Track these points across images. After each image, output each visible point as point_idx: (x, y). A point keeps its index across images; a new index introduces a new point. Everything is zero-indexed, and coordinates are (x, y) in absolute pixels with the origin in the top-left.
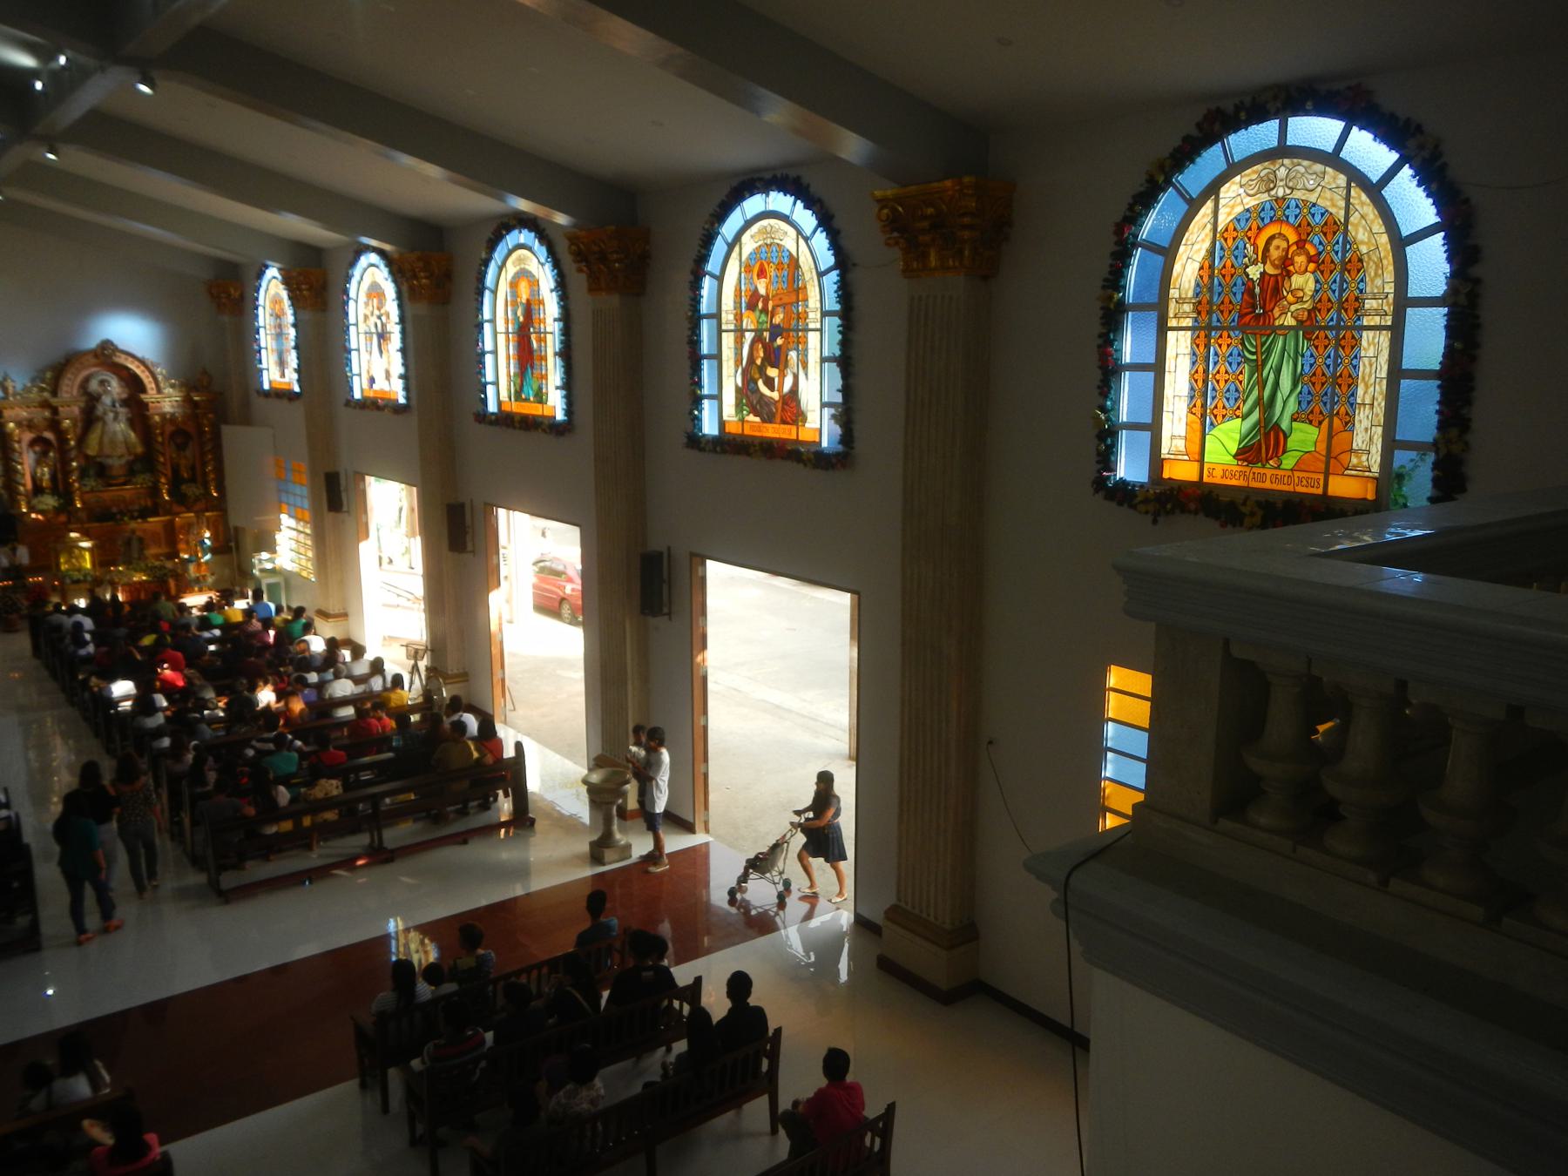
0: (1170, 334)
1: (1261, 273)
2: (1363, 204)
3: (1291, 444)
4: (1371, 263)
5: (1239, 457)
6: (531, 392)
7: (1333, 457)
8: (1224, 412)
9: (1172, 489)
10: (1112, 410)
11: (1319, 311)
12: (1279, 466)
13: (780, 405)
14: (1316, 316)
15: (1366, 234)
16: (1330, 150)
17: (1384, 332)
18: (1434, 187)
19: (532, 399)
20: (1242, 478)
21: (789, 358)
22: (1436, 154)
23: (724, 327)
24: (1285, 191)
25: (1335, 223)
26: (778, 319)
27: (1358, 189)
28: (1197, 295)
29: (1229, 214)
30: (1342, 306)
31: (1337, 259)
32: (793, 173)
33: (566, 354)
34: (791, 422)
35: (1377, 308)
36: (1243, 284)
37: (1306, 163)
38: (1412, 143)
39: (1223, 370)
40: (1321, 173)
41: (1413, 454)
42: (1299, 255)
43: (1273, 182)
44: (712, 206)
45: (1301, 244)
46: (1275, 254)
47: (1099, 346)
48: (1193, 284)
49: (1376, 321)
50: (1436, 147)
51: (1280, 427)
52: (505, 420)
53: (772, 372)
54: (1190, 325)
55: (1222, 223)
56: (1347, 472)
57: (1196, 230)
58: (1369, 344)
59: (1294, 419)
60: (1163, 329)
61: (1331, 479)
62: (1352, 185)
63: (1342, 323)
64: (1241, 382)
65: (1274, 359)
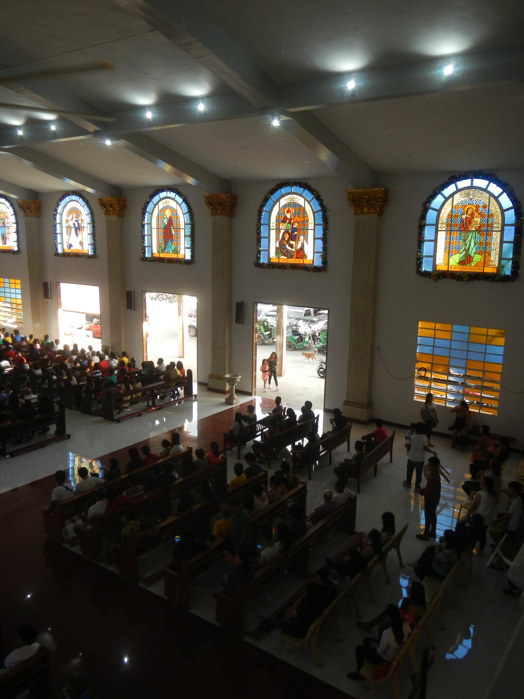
0: (439, 232)
1: (466, 217)
2: (493, 201)
3: (473, 260)
6: (170, 250)
7: (485, 263)
8: (455, 252)
9: (441, 272)
10: (422, 252)
11: (482, 227)
13: (295, 253)
16: (485, 188)
17: (499, 232)
18: (512, 198)
19: (171, 252)
21: (300, 238)
22: (512, 191)
23: (271, 228)
25: (486, 205)
26: (295, 226)
27: (492, 198)
28: (447, 222)
30: (488, 226)
31: (487, 214)
32: (304, 181)
33: (193, 236)
34: (300, 258)
35: (497, 226)
36: (460, 220)
37: (478, 190)
38: (507, 188)
39: (455, 241)
41: (506, 261)
42: (476, 213)
43: (469, 194)
44: (269, 189)
46: (469, 212)
47: (418, 235)
48: (446, 219)
49: (497, 229)
50: (512, 189)
51: (471, 255)
52: (154, 260)
53: (292, 242)
54: (445, 230)
58: (495, 235)
59: (475, 253)
60: (437, 231)
61: (485, 268)
62: (491, 196)
64: (460, 244)
65: (469, 239)
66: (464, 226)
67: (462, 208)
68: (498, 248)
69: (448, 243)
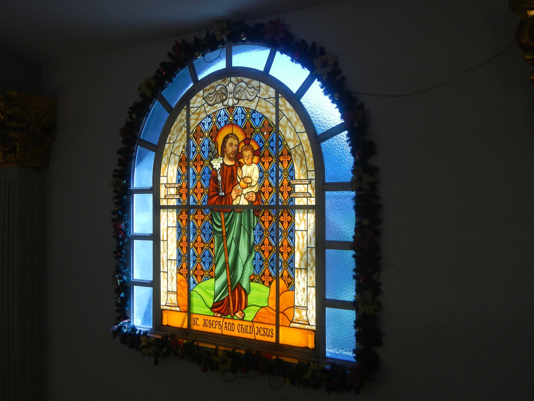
2: (288, 110)
4: (297, 156)
5: (215, 310)
12: (243, 318)
14: (261, 198)
15: (292, 133)
20: (217, 326)
24: (233, 102)
25: (270, 125)
27: (284, 99)
28: (179, 181)
29: (197, 120)
36: (210, 173)
37: (246, 80)
40: (257, 87)
42: (246, 150)
43: (225, 95)
45: (247, 141)
46: (230, 149)
50: (336, 64)
51: (241, 286)
54: (175, 204)
55: (193, 126)
56: (292, 325)
57: (175, 132)
58: (301, 221)
62: (280, 95)
63: (280, 204)
64: (212, 249)
65: (233, 233)
66: (218, 190)
67: (212, 138)
68: (312, 265)
69: (184, 244)
